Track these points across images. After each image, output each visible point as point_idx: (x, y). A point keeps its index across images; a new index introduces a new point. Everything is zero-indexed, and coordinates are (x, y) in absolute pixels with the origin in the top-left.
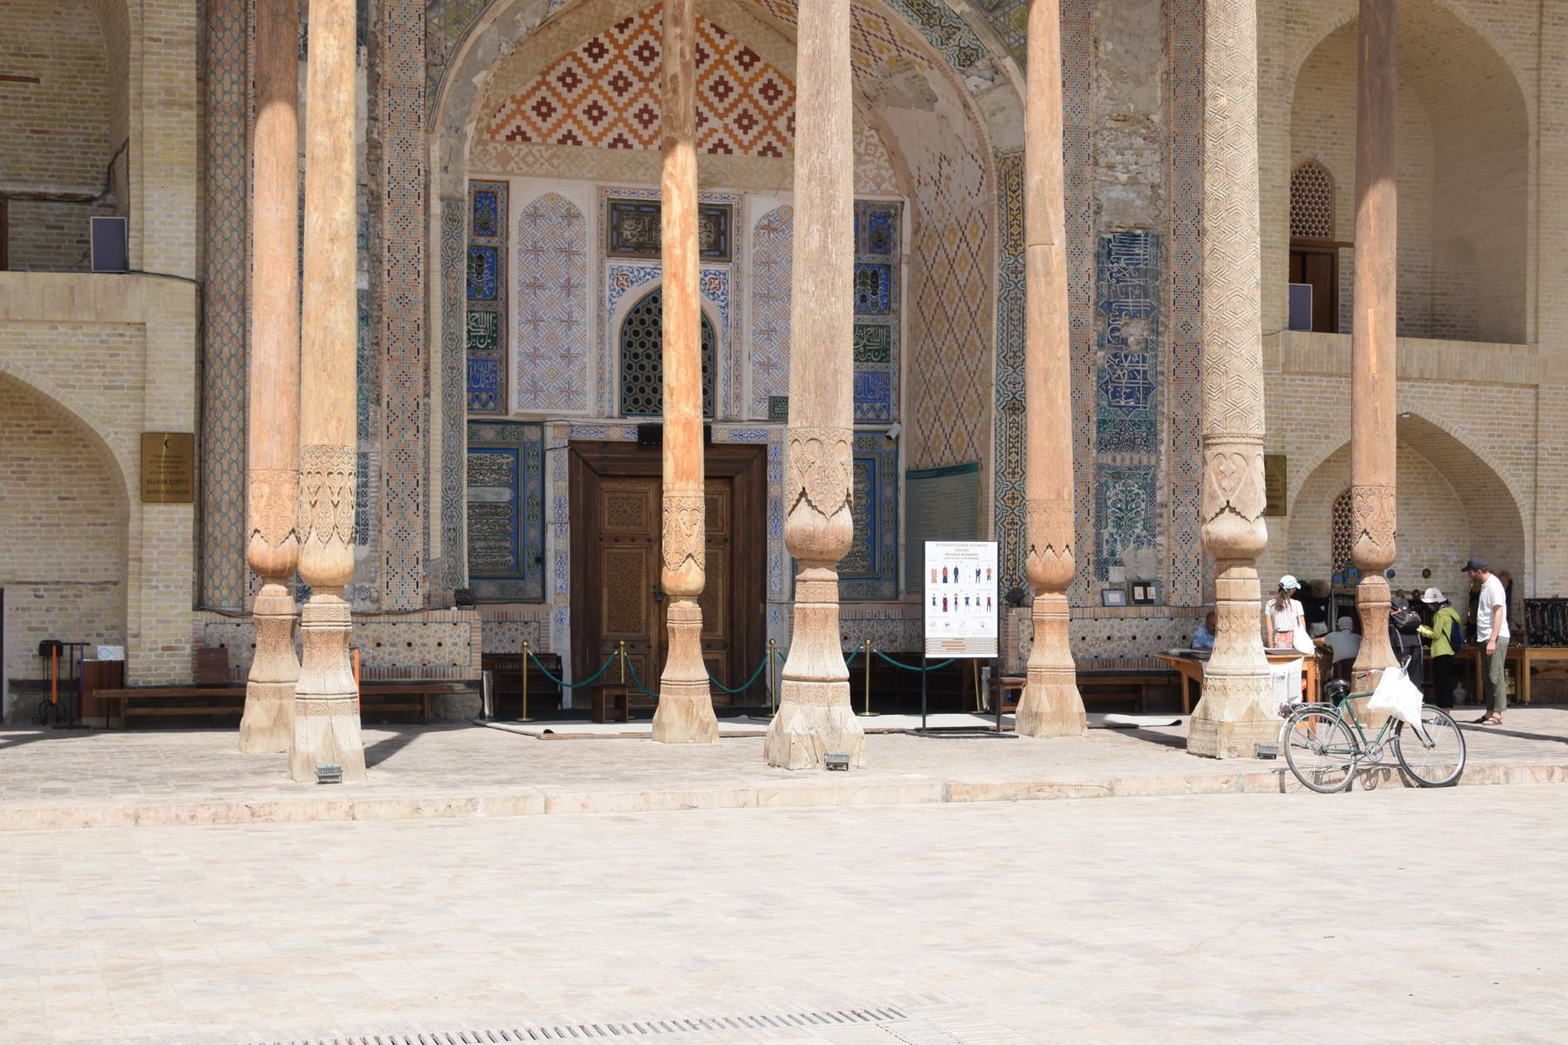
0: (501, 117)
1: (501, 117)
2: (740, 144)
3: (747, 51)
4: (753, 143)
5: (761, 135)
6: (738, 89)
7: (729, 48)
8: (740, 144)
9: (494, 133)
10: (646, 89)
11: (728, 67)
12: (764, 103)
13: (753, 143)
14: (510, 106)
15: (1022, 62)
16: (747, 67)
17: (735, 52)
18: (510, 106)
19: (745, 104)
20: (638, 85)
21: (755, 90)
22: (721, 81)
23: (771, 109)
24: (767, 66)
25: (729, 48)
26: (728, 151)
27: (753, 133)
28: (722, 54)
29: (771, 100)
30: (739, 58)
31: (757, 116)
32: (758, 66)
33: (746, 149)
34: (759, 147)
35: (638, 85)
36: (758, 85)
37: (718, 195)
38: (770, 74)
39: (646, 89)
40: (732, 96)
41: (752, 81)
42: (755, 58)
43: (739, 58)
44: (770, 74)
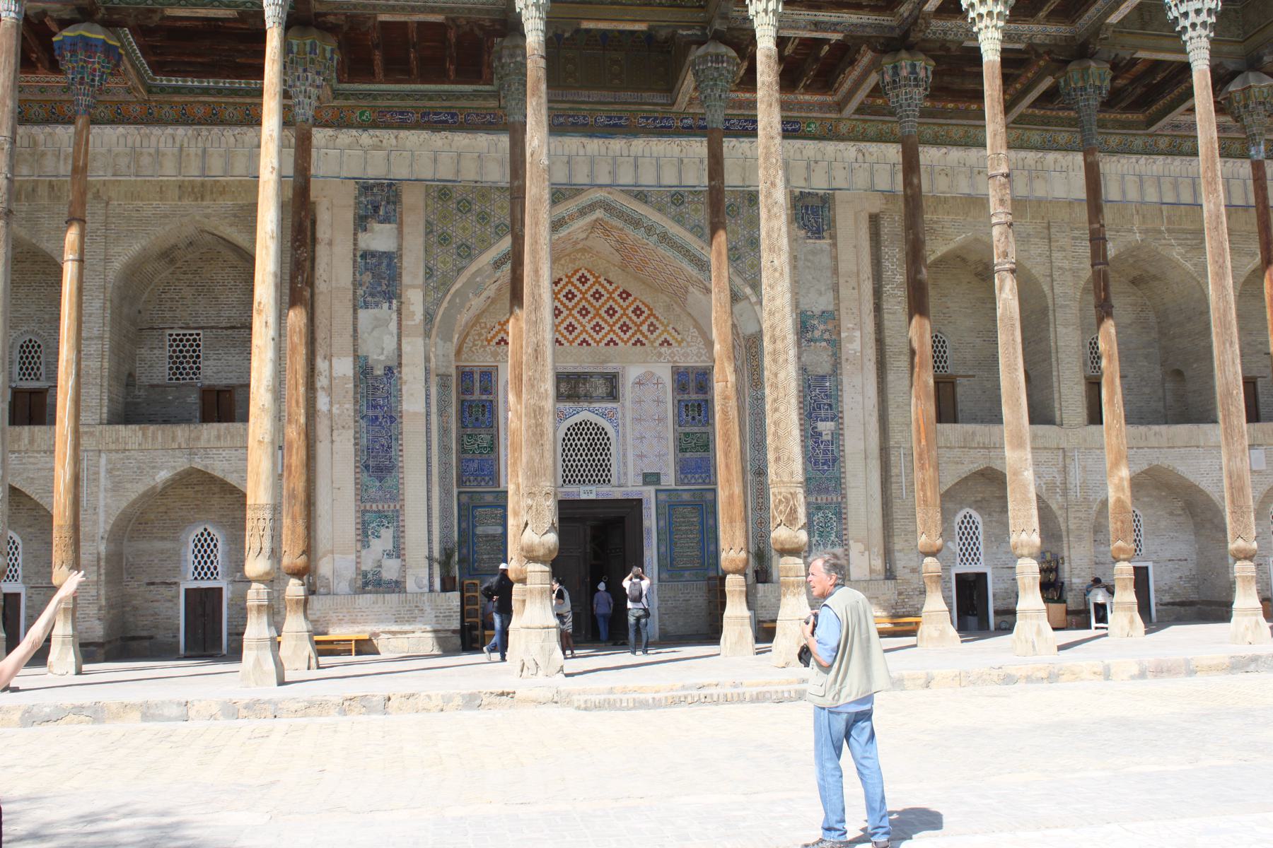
0: (493, 333)
1: (493, 333)
2: (622, 340)
3: (624, 292)
4: (629, 339)
5: (633, 335)
6: (620, 312)
7: (614, 290)
8: (622, 340)
9: (489, 341)
10: (570, 314)
11: (614, 300)
12: (634, 318)
13: (629, 339)
14: (498, 327)
15: (756, 285)
16: (625, 300)
17: (618, 292)
18: (498, 327)
19: (625, 319)
20: (566, 312)
21: (629, 312)
22: (611, 308)
23: (638, 321)
24: (635, 299)
25: (614, 290)
26: (616, 344)
27: (629, 334)
28: (611, 294)
29: (638, 316)
30: (620, 295)
31: (631, 325)
32: (631, 299)
33: (626, 343)
34: (633, 341)
35: (566, 312)
36: (631, 309)
37: (610, 368)
38: (638, 303)
39: (570, 314)
40: (617, 315)
41: (628, 307)
42: (628, 295)
43: (620, 295)
44: (638, 303)
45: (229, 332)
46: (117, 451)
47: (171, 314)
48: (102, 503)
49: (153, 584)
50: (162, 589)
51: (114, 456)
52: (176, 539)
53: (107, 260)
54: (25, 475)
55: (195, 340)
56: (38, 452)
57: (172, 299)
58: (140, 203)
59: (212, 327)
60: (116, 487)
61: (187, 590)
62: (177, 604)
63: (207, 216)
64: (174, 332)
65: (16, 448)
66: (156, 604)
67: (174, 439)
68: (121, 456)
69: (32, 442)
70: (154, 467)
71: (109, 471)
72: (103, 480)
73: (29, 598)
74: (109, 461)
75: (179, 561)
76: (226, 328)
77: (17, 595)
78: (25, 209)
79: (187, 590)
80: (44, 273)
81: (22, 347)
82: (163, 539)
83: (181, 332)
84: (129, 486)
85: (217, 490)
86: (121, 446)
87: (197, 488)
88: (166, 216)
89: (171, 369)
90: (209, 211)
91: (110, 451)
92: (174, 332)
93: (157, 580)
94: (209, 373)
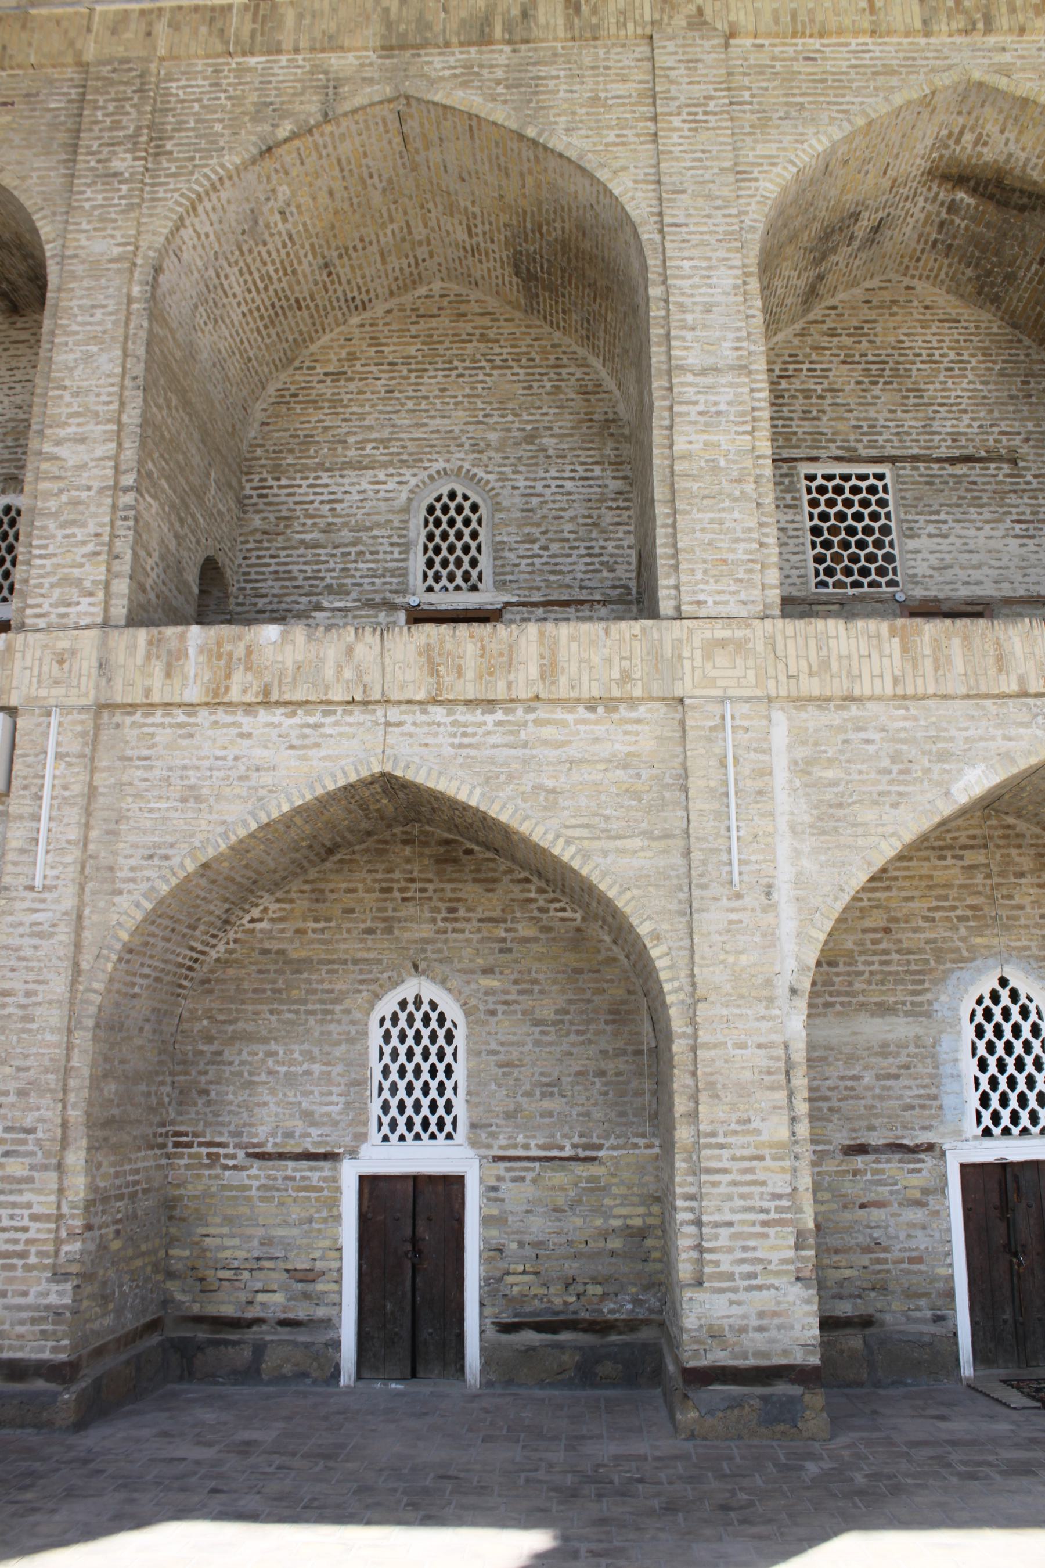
45: (960, 469)
46: (822, 701)
47: (808, 426)
48: (784, 875)
49: (862, 1149)
50: (892, 1167)
51: (812, 718)
52: (921, 1012)
53: (741, 174)
54: (528, 782)
55: (872, 490)
56: (569, 703)
57: (807, 393)
58: (816, 43)
59: (915, 458)
60: (829, 818)
61: (966, 1169)
62: (940, 1214)
63: (1005, 71)
64: (820, 470)
65: (500, 692)
66: (877, 1214)
67: (1001, 663)
68: (836, 718)
69: (550, 670)
70: (943, 757)
71: (802, 768)
72: (786, 801)
73: (491, 1190)
74: (798, 737)
75: (935, 1079)
76: (953, 461)
77: (454, 1184)
78: (502, 60)
79: (966, 1169)
80: (483, 338)
81: (431, 510)
82: (884, 1010)
83: (838, 469)
84: (869, 815)
85: (1026, 863)
86: (837, 687)
87: (972, 857)
88: (891, 72)
89: (819, 559)
90: (1007, 58)
91: (799, 701)
92: (820, 470)
93: (876, 1139)
94: (921, 568)
